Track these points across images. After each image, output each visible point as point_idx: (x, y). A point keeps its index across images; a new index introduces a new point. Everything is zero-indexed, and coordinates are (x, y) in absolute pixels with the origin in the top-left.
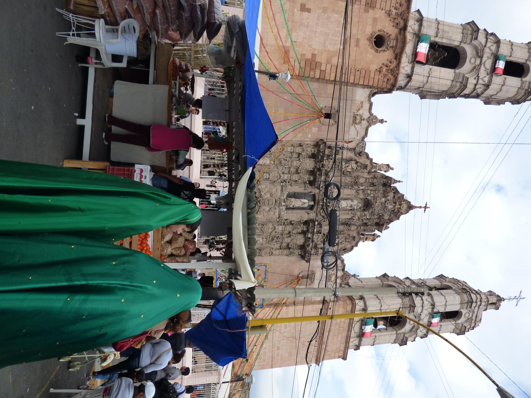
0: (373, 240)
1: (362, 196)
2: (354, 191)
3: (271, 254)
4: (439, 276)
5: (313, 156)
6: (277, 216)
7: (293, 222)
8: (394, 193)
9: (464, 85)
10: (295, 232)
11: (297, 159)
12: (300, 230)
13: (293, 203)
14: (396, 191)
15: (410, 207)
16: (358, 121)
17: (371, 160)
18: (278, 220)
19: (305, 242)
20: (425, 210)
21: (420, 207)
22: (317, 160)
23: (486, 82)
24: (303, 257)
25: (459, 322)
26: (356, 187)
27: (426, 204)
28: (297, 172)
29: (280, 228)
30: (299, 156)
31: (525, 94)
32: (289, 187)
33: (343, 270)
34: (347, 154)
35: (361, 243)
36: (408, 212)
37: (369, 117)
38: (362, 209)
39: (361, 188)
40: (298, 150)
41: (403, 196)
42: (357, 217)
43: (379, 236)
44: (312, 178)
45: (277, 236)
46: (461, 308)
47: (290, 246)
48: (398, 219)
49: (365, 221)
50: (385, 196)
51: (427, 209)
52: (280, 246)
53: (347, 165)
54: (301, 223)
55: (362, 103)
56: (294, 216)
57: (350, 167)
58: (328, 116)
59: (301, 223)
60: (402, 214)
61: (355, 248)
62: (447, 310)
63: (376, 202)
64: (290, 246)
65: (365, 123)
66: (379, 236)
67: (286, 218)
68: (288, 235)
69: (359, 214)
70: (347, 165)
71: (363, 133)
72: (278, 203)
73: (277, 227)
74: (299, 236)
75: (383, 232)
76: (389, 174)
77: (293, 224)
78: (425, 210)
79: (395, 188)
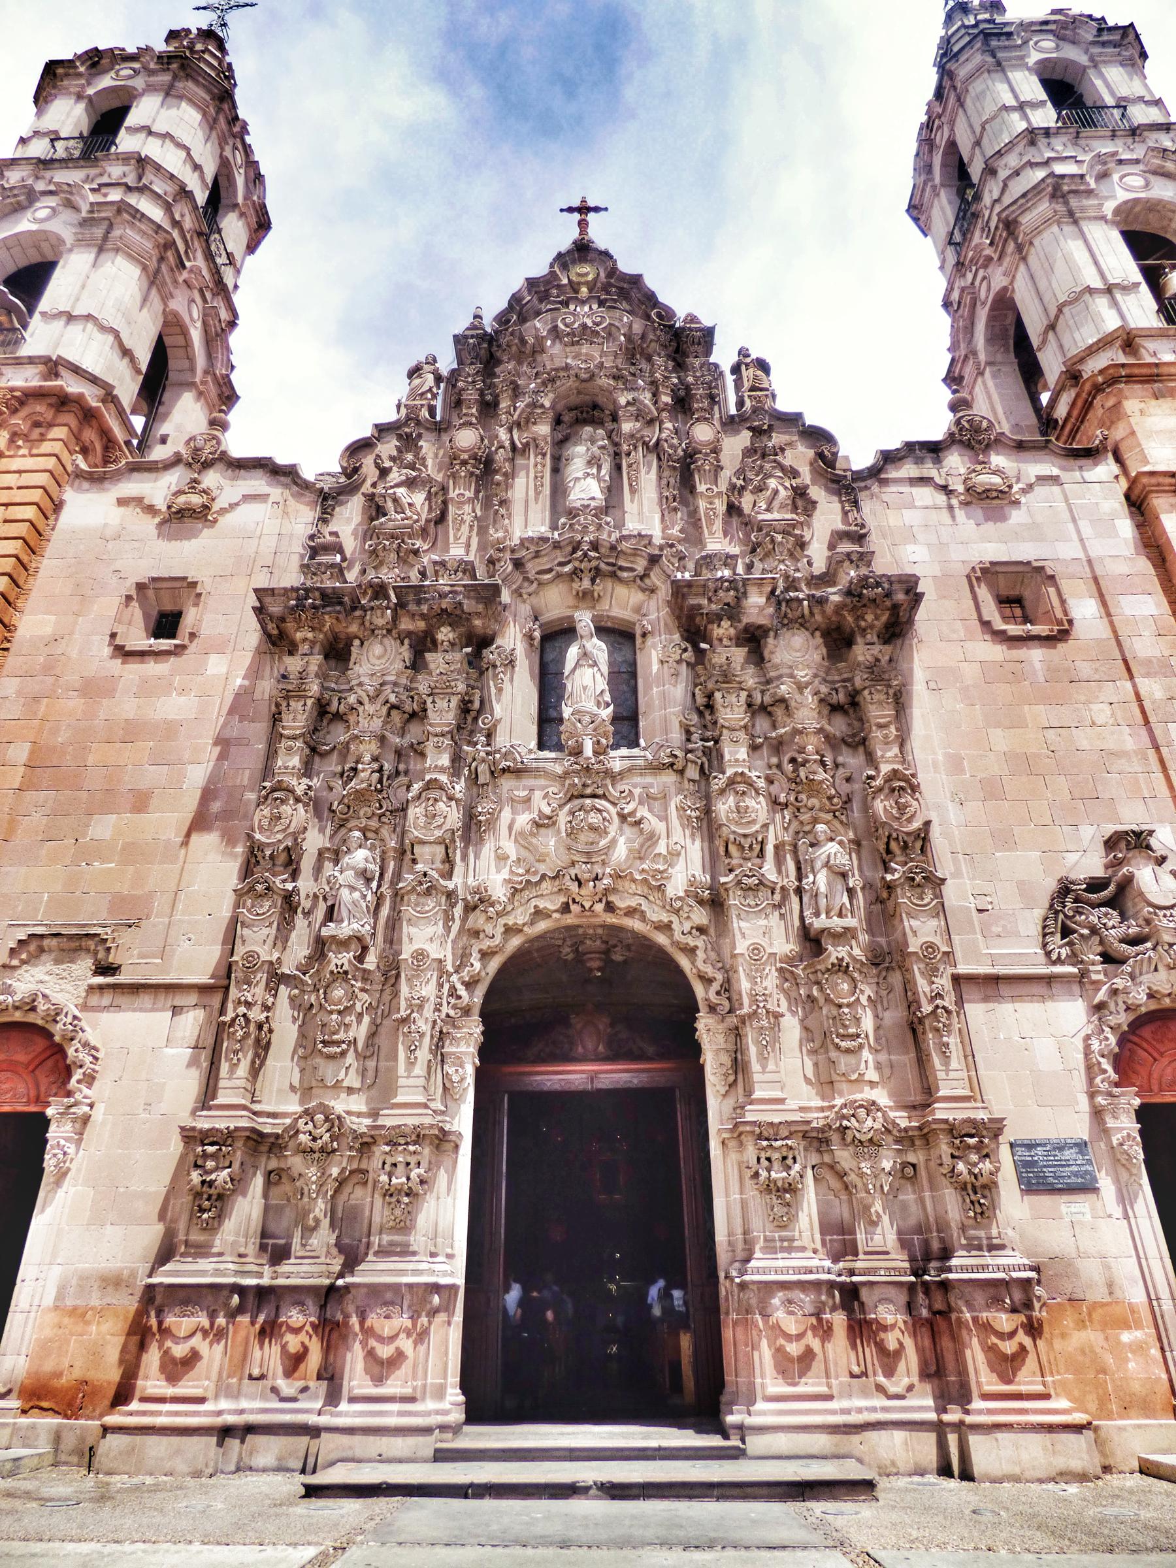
0: (763, 365)
1: (543, 429)
2: (520, 461)
3: (903, 784)
4: (916, 220)
5: (338, 653)
6: (669, 778)
7: (701, 700)
8: (523, 319)
9: (119, 211)
10: (750, 678)
11: (352, 719)
12: (739, 654)
13: (590, 706)
14: (517, 310)
15: (582, 250)
16: (196, 500)
17: (382, 430)
18: (692, 772)
19: (802, 623)
20: (597, 209)
21: (583, 224)
22: (354, 628)
23: (126, 168)
24: (897, 628)
25: (1083, 59)
26: (501, 456)
27: (570, 210)
28: (418, 715)
29: (736, 754)
30: (338, 717)
31: (188, 76)
32: (502, 740)
33: (934, 449)
34: (348, 521)
35: (784, 405)
36: (606, 254)
37: (189, 465)
38: (610, 426)
39: (503, 435)
40: (297, 719)
41: (531, 283)
42: (646, 432)
43: (743, 353)
44: (445, 634)
45: (789, 768)
46: (1021, 64)
47: (841, 697)
48: (636, 280)
49: (666, 399)
50: (539, 349)
51: (591, 204)
52: (853, 746)
53: (390, 505)
54: (701, 653)
55: (121, 502)
56: (665, 694)
57: (401, 491)
58: (166, 624)
59: (701, 653)
60: (613, 272)
61: (809, 420)
62: (1043, 96)
63: (567, 367)
64: (841, 697)
65: (212, 479)
66: (743, 353)
67: (677, 736)
68: (779, 712)
69: (627, 427)
70: (390, 505)
71: (257, 483)
72: (587, 786)
73: (730, 772)
74: (777, 659)
75: (707, 322)
76: (447, 362)
77: (710, 696)
78: (597, 209)
79: (502, 319)
